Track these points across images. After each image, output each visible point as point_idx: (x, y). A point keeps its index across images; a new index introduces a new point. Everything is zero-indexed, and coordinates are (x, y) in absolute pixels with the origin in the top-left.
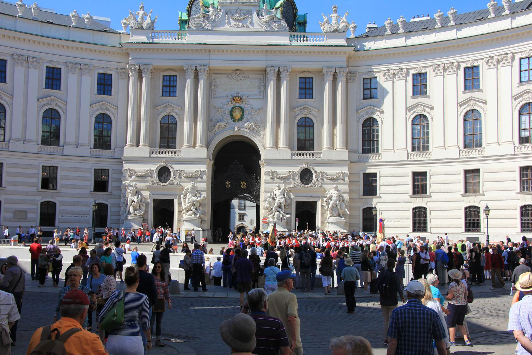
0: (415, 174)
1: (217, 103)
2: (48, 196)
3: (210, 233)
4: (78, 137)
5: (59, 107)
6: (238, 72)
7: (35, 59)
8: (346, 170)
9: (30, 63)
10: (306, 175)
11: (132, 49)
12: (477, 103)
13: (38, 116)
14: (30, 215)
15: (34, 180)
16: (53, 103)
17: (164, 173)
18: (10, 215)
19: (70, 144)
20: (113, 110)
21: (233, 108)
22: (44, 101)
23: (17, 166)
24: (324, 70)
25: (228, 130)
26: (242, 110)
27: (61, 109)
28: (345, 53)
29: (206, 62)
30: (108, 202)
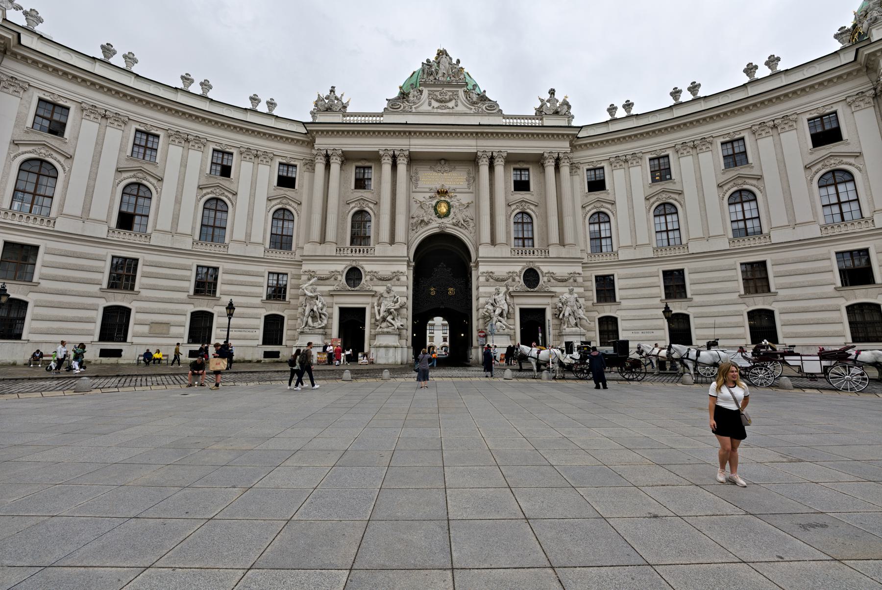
0: (666, 274)
1: (420, 197)
3: (411, 351)
6: (443, 162)
8: (578, 269)
10: (531, 277)
11: (317, 131)
12: (747, 181)
14: (174, 330)
17: (354, 275)
18: (145, 329)
20: (295, 206)
21: (438, 202)
24: (546, 155)
25: (433, 228)
26: (448, 203)
27: (229, 199)
28: (568, 135)
29: (404, 148)
30: (285, 314)
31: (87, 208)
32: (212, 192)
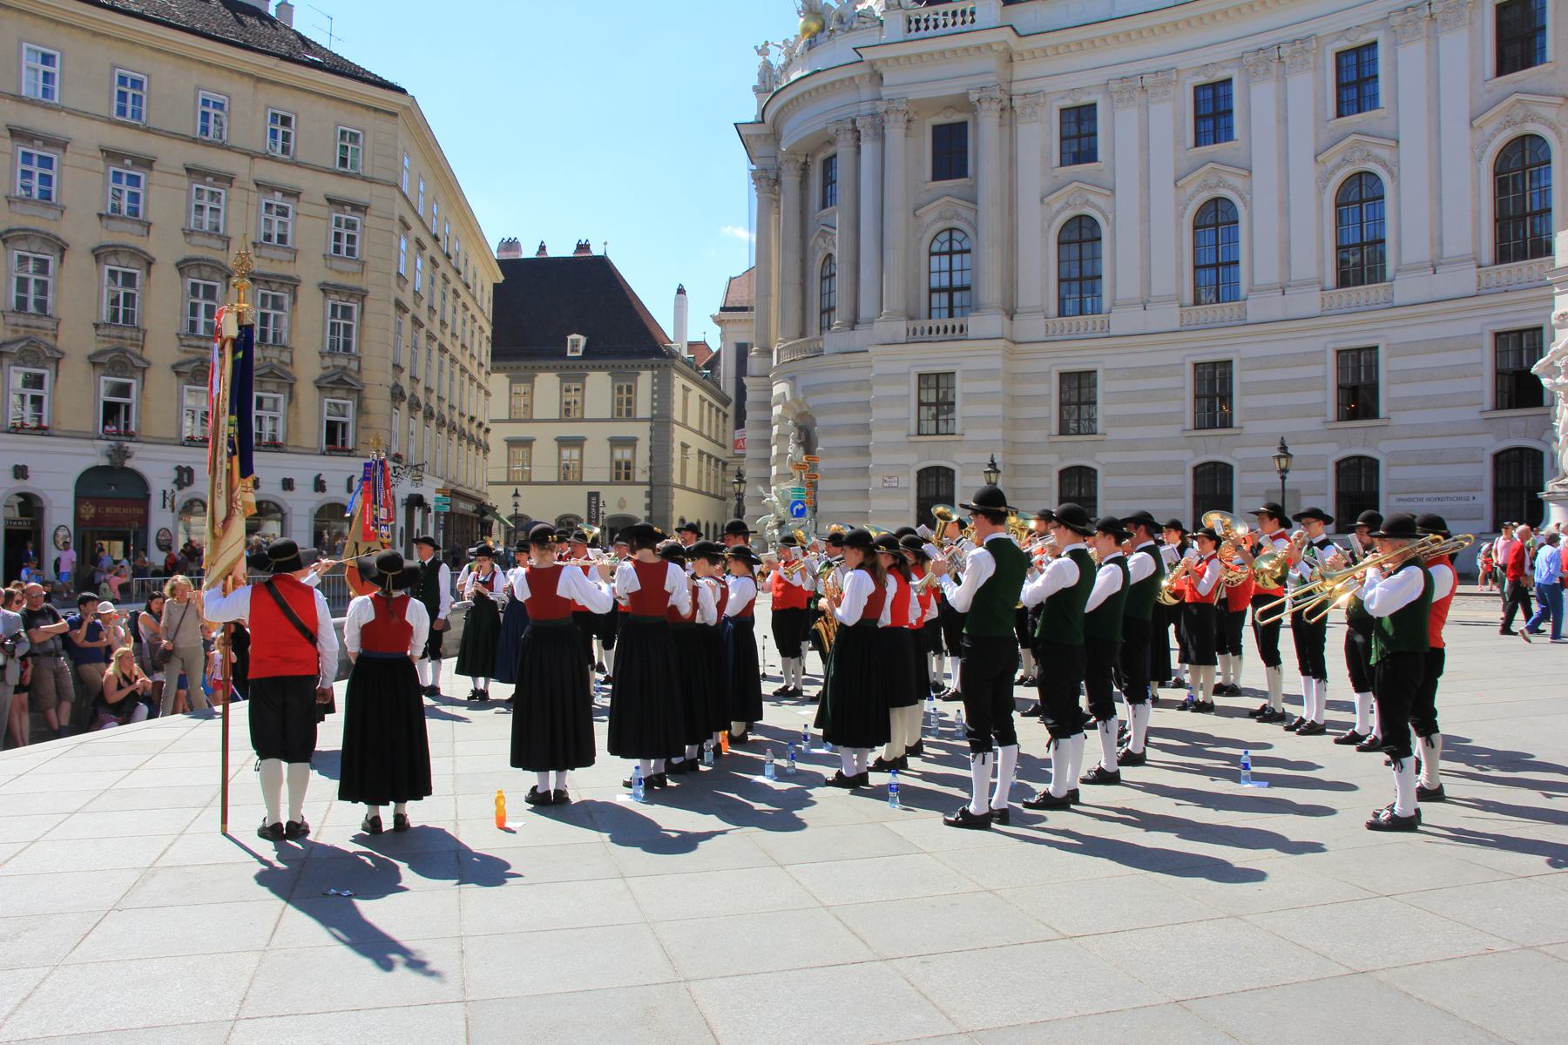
2: (1358, 439)
4: (1438, 241)
5: (1377, 160)
7: (1298, 45)
9: (1288, 61)
13: (1320, 207)
15: (1314, 397)
16: (1358, 154)
19: (1416, 268)
22: (1333, 157)
23: (1266, 362)
27: (1384, 165)
31: (1146, 280)
32: (1346, 161)
